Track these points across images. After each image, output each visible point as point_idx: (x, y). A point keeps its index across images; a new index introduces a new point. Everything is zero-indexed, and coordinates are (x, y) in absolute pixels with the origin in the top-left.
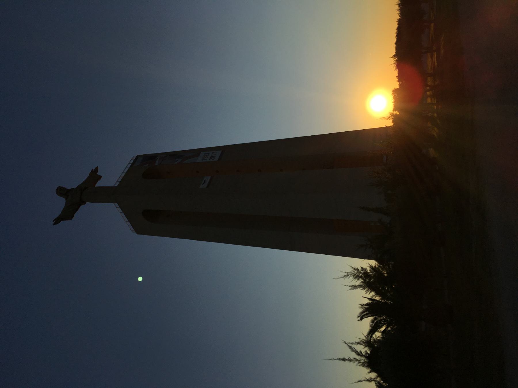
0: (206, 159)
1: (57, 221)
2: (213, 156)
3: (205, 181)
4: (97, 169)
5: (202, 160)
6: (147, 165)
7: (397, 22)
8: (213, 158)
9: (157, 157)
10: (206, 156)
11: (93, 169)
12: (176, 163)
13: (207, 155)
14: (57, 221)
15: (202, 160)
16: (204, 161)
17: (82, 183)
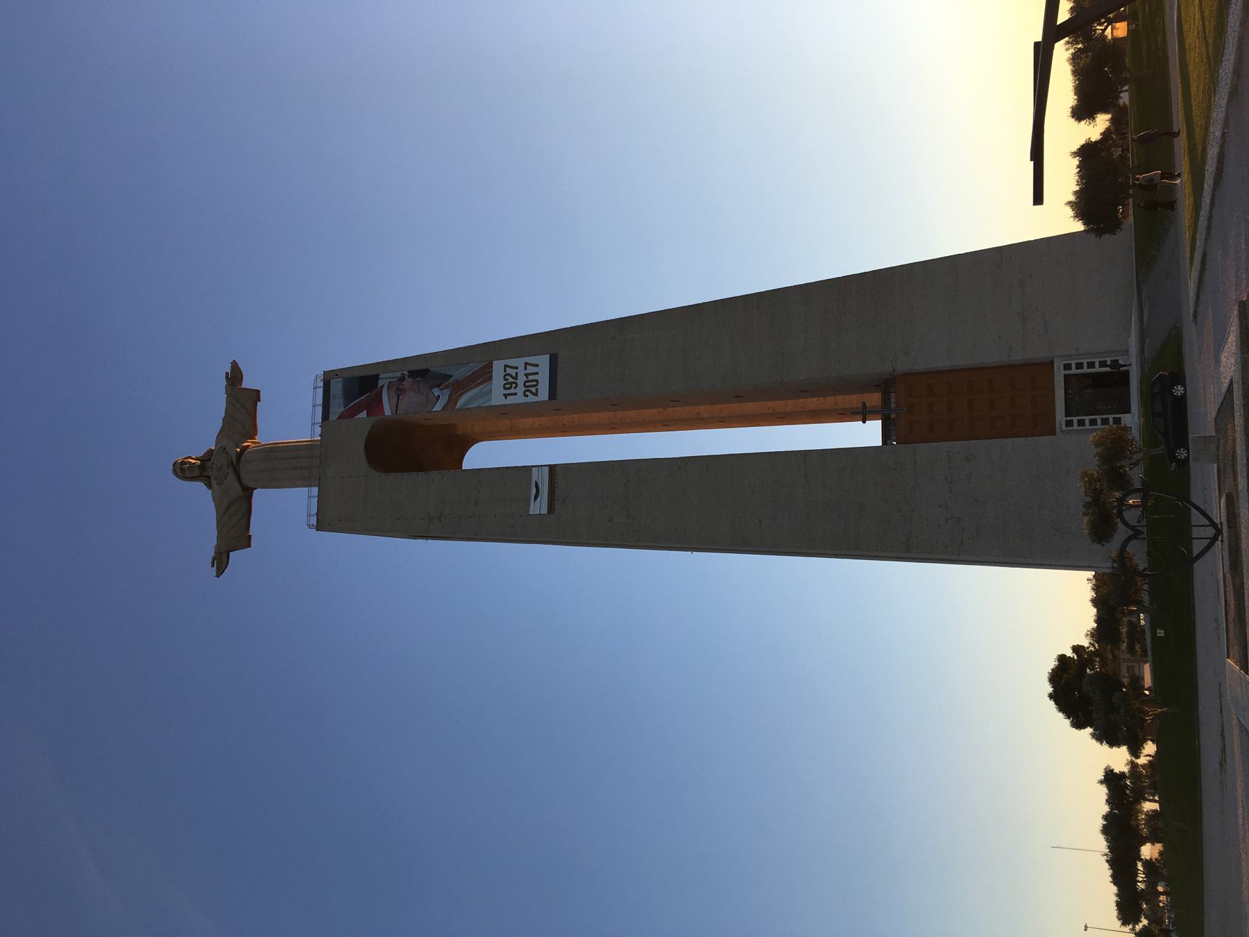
0: (516, 394)
1: (221, 562)
2: (530, 378)
3: (536, 482)
4: (235, 366)
5: (506, 396)
6: (364, 414)
7: (1080, 222)
8: (533, 389)
9: (379, 386)
10: (511, 380)
11: (227, 373)
12: (438, 407)
13: (513, 372)
14: (221, 562)
15: (506, 396)
16: (511, 400)
17: (222, 427)
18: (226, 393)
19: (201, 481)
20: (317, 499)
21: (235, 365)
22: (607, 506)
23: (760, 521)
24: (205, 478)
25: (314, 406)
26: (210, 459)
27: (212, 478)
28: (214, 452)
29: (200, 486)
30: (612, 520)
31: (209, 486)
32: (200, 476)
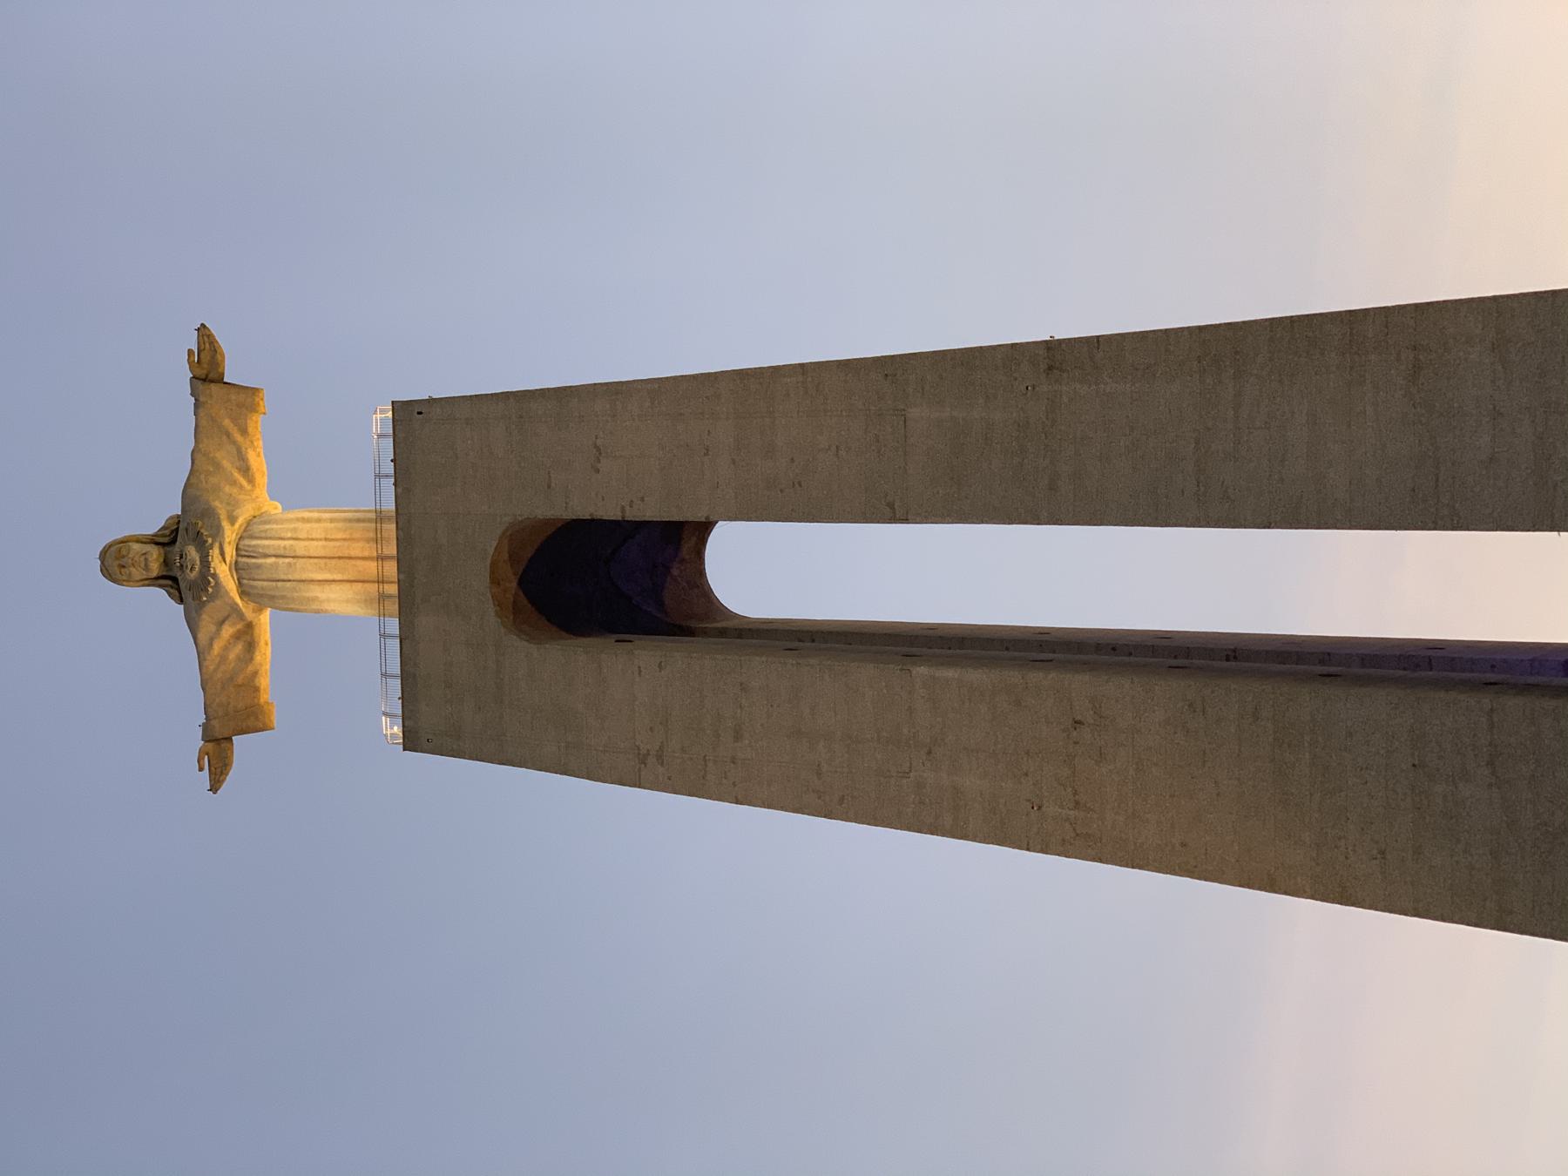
11: (190, 352)
18: (192, 395)
19: (160, 586)
20: (399, 681)
21: (202, 330)
22: (1026, 775)
23: (1383, 853)
24: (169, 582)
25: (378, 476)
26: (173, 542)
27: (182, 585)
28: (182, 526)
29: (159, 595)
30: (1040, 808)
31: (181, 601)
32: (157, 578)
